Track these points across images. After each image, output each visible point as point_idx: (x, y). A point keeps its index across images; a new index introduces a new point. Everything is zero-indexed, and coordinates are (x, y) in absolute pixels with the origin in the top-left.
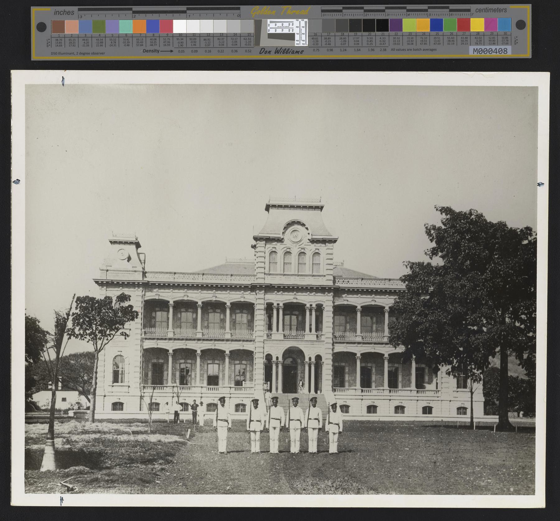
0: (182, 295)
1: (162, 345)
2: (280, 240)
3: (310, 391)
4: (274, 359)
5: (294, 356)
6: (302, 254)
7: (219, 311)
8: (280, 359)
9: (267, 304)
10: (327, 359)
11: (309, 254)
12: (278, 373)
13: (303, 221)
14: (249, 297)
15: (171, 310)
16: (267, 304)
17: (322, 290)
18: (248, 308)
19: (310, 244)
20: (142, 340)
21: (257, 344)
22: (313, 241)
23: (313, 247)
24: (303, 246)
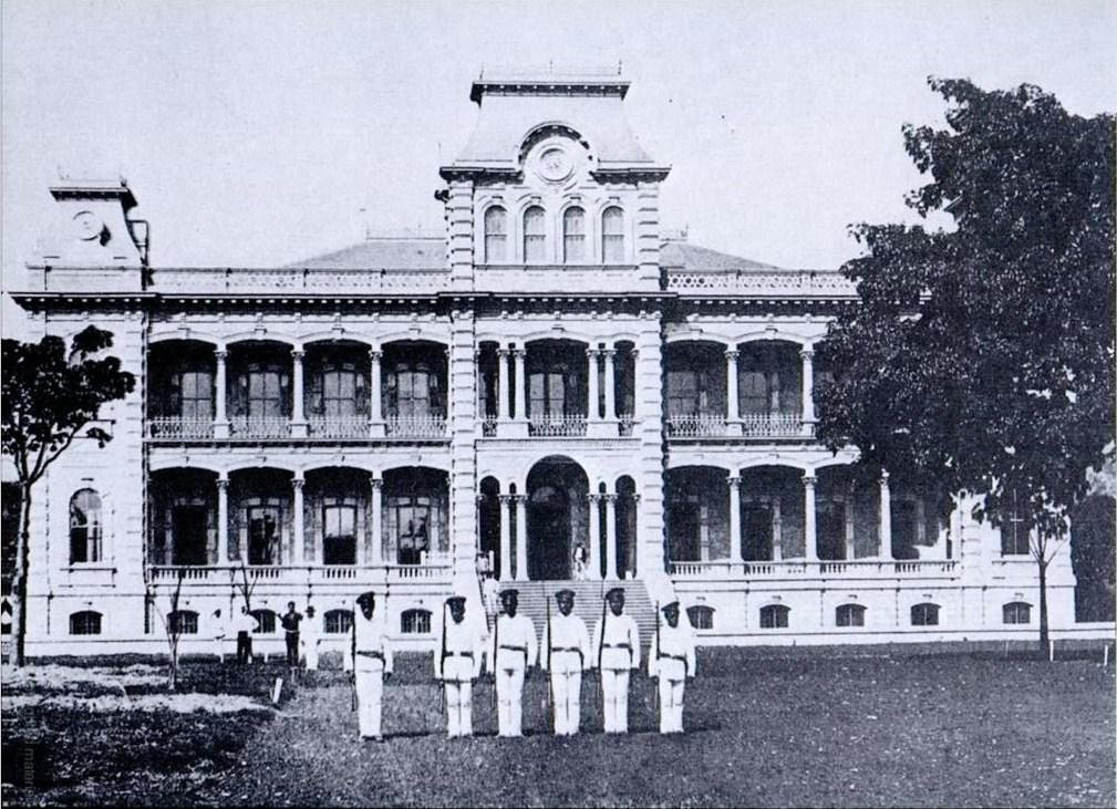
0: (252, 327)
1: (200, 459)
2: (513, 178)
3: (604, 573)
4: (504, 490)
5: (557, 482)
6: (573, 210)
7: (351, 367)
8: (521, 490)
9: (482, 344)
10: (648, 486)
11: (593, 211)
12: (515, 529)
13: (573, 126)
14: (431, 328)
15: (221, 368)
16: (482, 344)
17: (631, 304)
18: (430, 357)
19: (595, 184)
20: (147, 448)
21: (458, 453)
22: (601, 177)
23: (604, 192)
24: (575, 190)
